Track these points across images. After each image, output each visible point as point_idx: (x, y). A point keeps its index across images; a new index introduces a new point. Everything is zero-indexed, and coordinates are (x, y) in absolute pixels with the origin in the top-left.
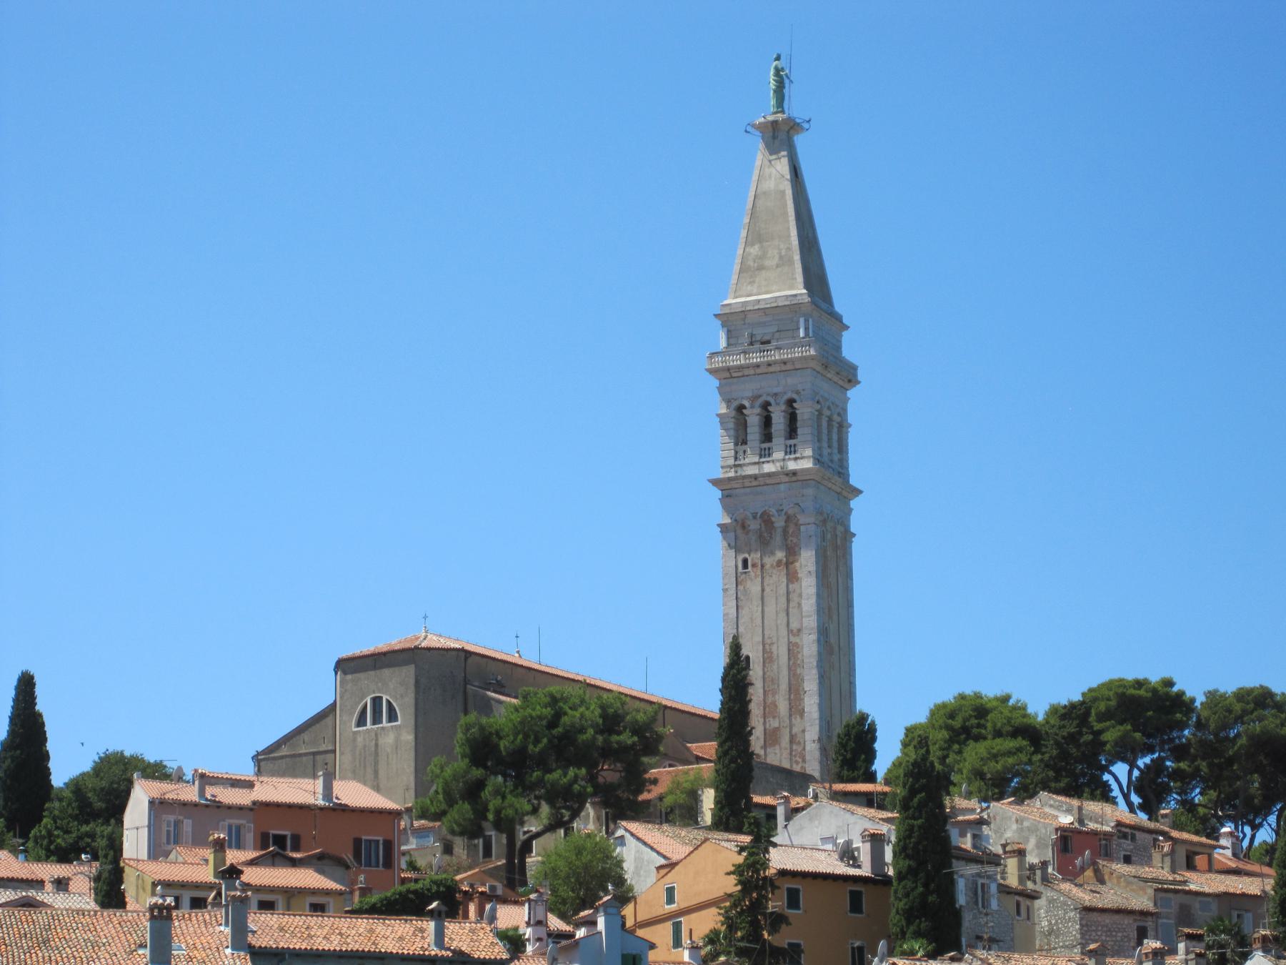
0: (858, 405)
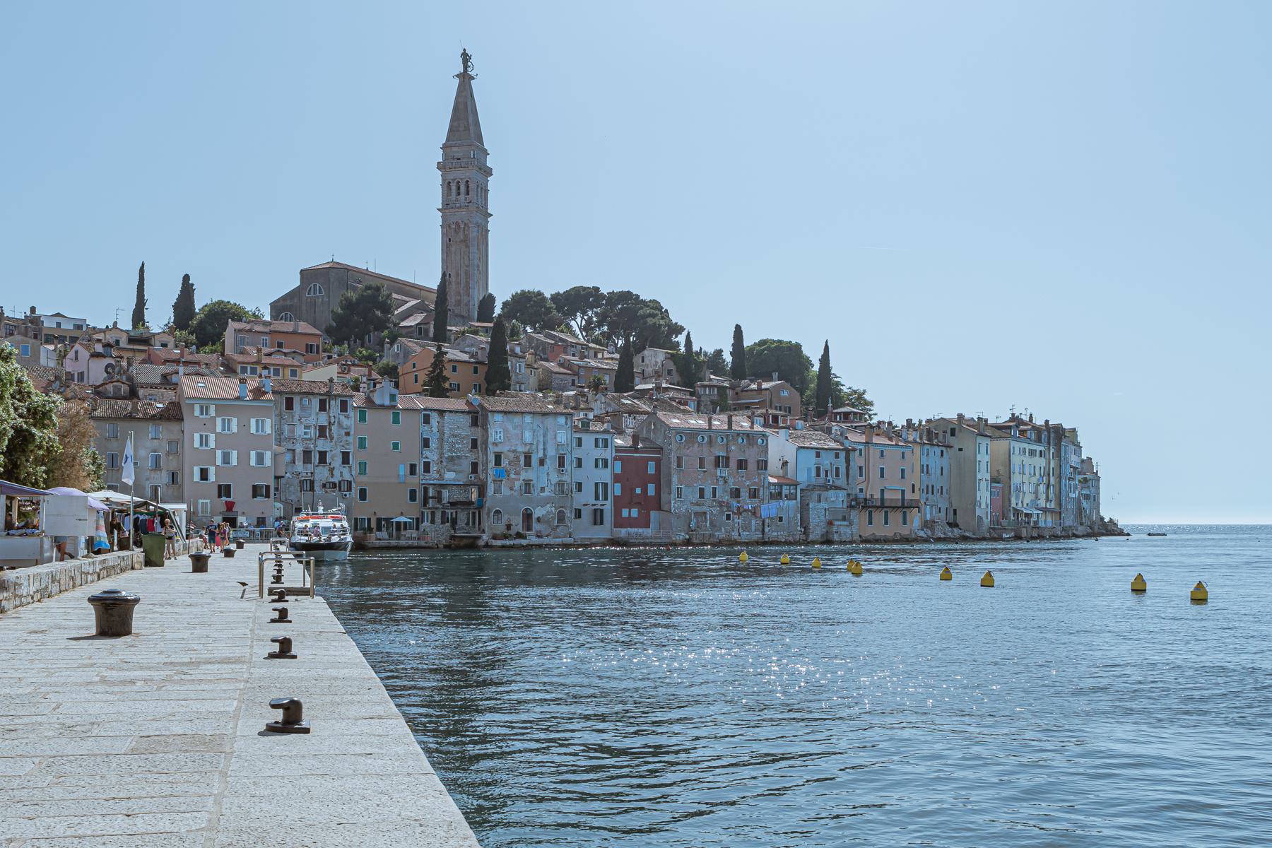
0: (492, 182)
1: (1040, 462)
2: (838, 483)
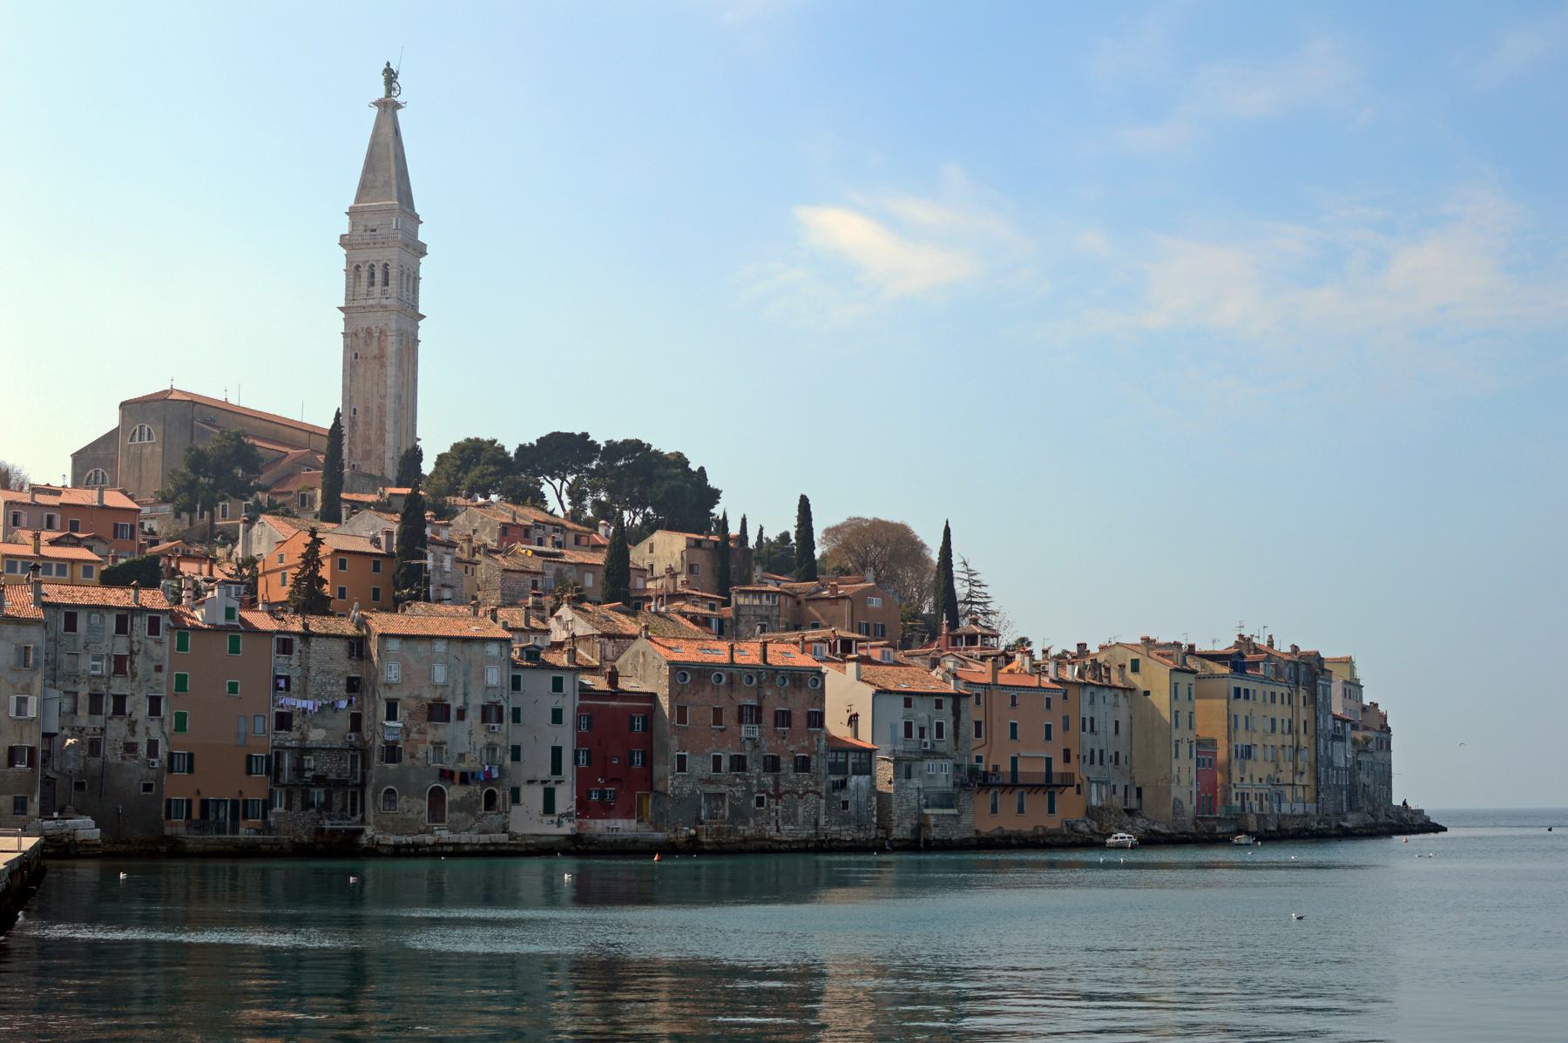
0: (426, 266)
1: (1281, 712)
2: (941, 747)
